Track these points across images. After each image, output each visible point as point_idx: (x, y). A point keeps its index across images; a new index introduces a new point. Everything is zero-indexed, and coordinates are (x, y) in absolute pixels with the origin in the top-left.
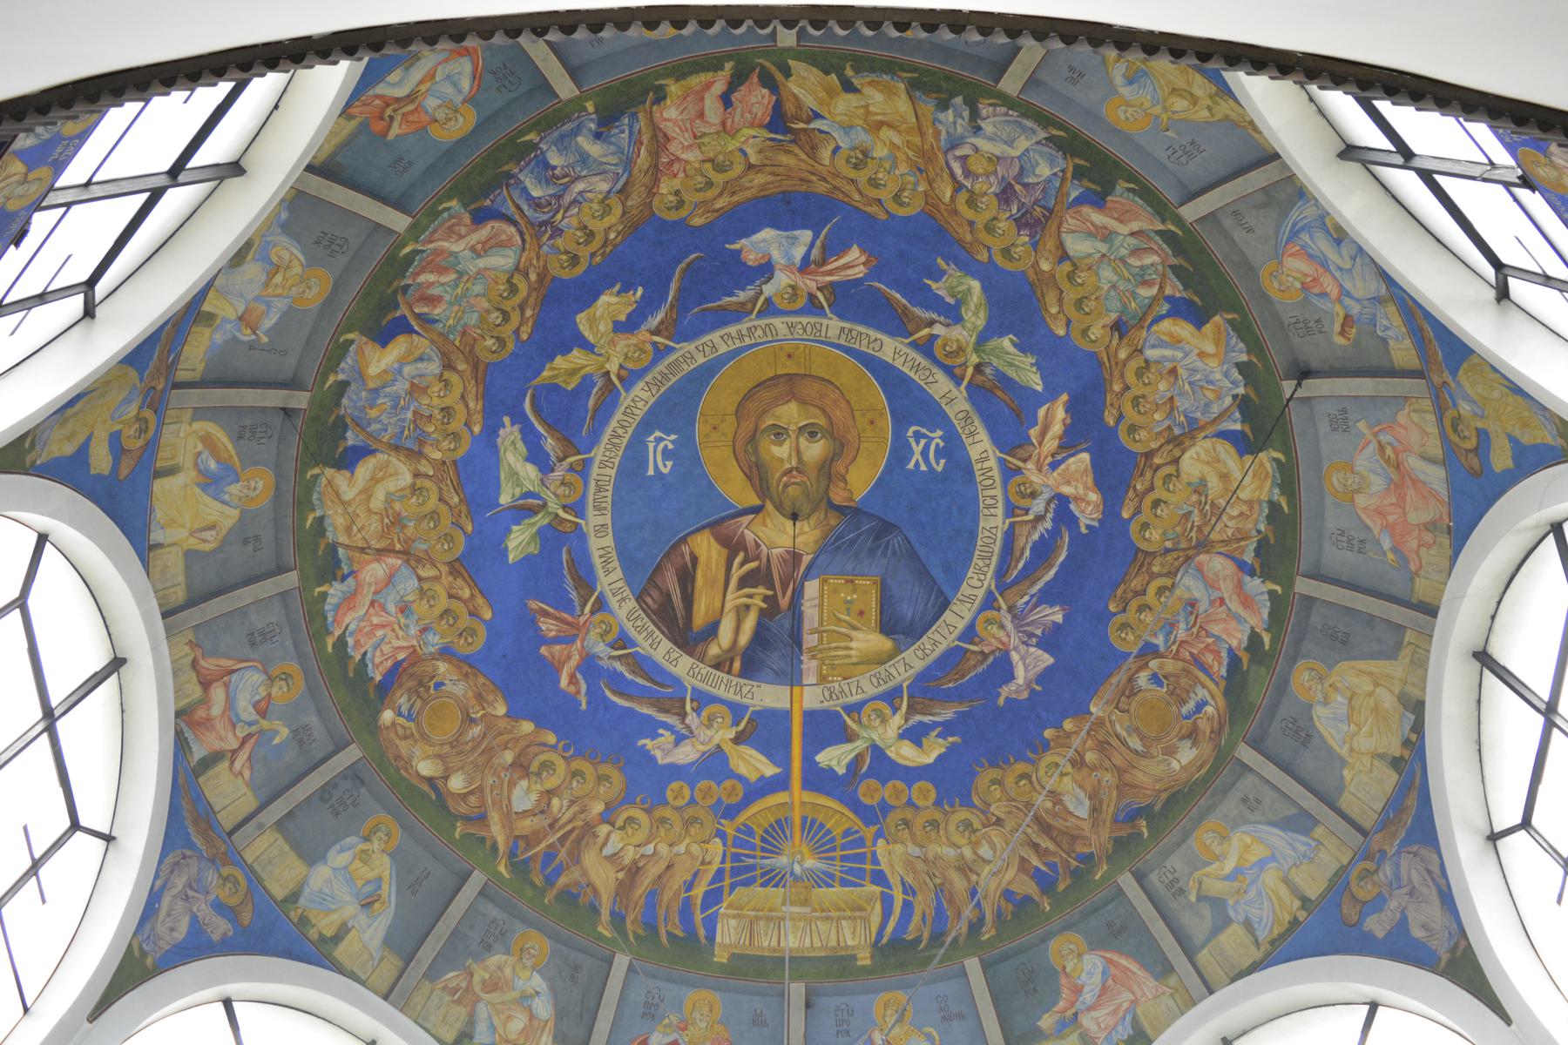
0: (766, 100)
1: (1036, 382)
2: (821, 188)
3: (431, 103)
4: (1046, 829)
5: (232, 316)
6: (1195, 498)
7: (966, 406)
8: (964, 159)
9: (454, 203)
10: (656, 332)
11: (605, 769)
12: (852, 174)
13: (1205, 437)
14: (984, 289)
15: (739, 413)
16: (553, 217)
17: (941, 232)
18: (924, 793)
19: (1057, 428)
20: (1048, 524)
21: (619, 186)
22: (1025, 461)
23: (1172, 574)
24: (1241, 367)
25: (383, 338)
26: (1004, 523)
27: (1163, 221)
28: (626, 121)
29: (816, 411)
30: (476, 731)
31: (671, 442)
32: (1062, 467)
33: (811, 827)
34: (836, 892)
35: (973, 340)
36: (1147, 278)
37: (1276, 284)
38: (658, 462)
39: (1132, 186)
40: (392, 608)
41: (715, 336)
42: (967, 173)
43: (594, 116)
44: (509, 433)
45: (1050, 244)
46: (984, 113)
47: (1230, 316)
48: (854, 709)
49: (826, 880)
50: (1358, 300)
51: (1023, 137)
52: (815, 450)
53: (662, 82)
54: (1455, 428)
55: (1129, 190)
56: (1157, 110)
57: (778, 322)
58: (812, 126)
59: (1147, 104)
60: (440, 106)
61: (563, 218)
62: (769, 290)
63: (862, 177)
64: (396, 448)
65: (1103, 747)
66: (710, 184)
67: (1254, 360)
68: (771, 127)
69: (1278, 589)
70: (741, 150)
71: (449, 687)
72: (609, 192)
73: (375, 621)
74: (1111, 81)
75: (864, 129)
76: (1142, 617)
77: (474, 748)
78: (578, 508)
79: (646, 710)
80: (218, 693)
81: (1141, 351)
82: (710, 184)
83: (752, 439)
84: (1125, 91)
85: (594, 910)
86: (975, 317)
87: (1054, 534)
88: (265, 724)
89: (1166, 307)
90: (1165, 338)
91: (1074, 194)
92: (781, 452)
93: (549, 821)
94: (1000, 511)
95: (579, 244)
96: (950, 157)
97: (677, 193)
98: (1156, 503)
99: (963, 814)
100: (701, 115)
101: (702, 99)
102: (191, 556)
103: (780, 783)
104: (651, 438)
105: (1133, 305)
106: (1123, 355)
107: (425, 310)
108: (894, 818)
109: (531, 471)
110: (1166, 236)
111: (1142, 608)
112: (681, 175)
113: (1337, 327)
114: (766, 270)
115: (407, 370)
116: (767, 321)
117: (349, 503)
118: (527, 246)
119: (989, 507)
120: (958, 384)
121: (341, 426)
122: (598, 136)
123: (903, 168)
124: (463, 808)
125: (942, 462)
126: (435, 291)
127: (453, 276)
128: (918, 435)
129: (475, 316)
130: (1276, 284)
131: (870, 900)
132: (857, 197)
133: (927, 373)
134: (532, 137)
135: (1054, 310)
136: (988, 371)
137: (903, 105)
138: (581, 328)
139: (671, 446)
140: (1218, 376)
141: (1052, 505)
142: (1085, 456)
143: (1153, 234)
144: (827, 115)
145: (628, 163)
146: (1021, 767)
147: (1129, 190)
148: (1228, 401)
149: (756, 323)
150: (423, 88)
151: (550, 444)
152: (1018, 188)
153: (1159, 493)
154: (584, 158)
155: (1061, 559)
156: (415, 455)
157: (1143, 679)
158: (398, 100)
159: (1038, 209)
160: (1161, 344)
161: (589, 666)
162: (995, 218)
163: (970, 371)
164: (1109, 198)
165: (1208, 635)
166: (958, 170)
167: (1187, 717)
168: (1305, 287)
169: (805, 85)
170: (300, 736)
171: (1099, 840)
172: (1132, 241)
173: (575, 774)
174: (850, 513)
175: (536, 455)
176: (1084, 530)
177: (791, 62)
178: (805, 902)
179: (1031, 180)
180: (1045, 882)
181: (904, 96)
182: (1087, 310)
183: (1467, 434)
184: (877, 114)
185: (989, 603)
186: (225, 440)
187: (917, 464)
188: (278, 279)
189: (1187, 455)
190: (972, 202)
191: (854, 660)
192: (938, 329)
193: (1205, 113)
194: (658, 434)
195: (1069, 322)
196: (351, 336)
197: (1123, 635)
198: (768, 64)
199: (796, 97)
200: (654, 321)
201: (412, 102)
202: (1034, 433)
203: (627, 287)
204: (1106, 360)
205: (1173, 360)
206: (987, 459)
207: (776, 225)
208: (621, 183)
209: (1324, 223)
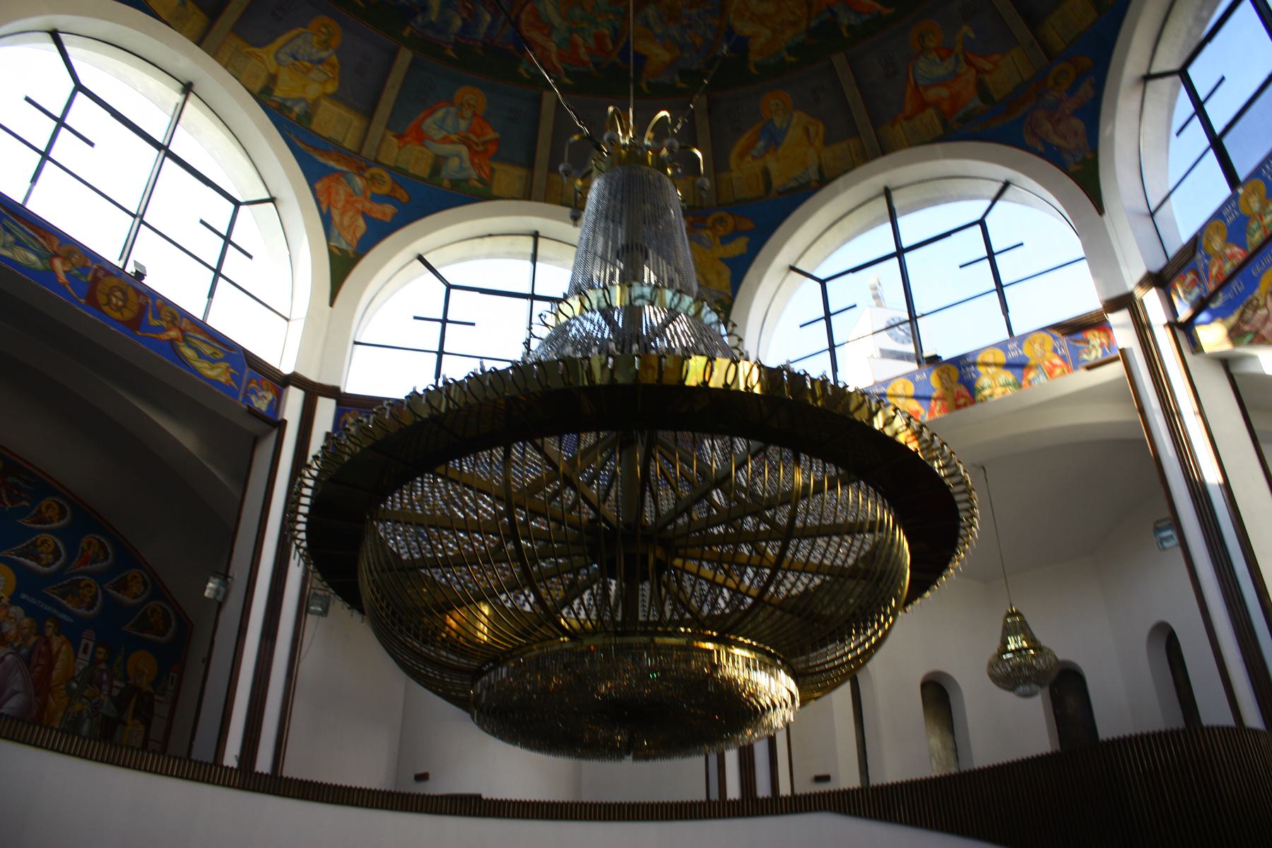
3: (463, 125)
25: (641, 59)
60: (464, 118)
80: (932, 94)
102: (827, 142)
107: (609, 42)
115: (659, 31)
126: (592, 42)
150: (454, 137)
158: (470, 148)
201: (468, 138)
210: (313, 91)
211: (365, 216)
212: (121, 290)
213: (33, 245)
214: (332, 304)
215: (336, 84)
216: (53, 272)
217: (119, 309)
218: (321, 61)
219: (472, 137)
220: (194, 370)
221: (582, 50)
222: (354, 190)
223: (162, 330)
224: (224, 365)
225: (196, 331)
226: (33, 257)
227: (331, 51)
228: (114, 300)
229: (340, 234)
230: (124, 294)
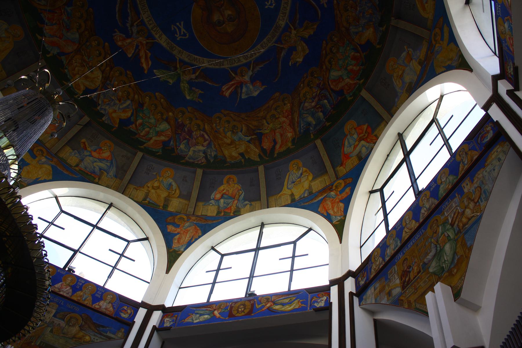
0: (264, 144)
3: (355, 136)
5: (414, 61)
6: (90, 64)
7: (175, 53)
8: (205, 140)
9: (349, 99)
13: (99, 86)
14: (186, 97)
16: (320, 92)
19: (143, 60)
20: (128, 25)
21: (302, 105)
22: (147, 43)
24: (103, 115)
26: (142, 17)
27: (145, 147)
28: (302, 131)
31: (267, 5)
32: (134, 48)
35: (182, 77)
36: (142, 126)
37: (108, 144)
39: (158, 154)
42: (203, 136)
43: (311, 132)
46: (204, 159)
47: (114, 129)
50: (86, 156)
51: (191, 155)
52: (216, 17)
53: (293, 147)
54: (41, 150)
55: (158, 152)
56: (161, 179)
58: (250, 138)
59: (164, 179)
60: (353, 135)
61: (317, 91)
62: (250, 73)
67: (101, 120)
68: (261, 134)
69: (48, 56)
70: (268, 124)
72: (305, 102)
74: (175, 182)
75: (235, 141)
76: (80, 13)
81: (132, 101)
82: (276, 109)
84: (171, 180)
86: (184, 86)
89: (132, 119)
90: (128, 110)
91: (172, 143)
92: (228, 12)
94: (146, 20)
95: (311, 81)
96: (209, 139)
97: (285, 104)
98: (100, 54)
100: (281, 135)
101: (282, 141)
104: (274, 5)
105: (141, 115)
106: (136, 96)
107: (356, 54)
110: (143, 143)
112: (284, 111)
113: (87, 144)
114: (253, 80)
116: (248, 60)
118: (327, 80)
120: (180, 60)
122: (309, 124)
123: (221, 130)
125: (173, 29)
126: (354, 62)
127: (349, 68)
128: (185, 35)
129: (341, 51)
130: (108, 144)
132: (232, 115)
133: (191, 59)
134: (328, 124)
135: (162, 100)
137: (226, 153)
138: (306, 47)
139: (266, 3)
140: (107, 108)
141: (130, 32)
142: (130, 56)
143: (146, 141)
144: (246, 143)
147: (158, 152)
148: (100, 102)
149: (251, 59)
152: (188, 137)
155: (117, 16)
158: (363, 140)
159: (180, 132)
160: (127, 107)
162: (190, 123)
163: (178, 66)
164: (162, 146)
166: (206, 136)
168: (101, 149)
169: (254, 153)
172: (150, 136)
176: (116, 30)
177: (259, 160)
181: (227, 156)
182: (153, 106)
183: (38, 153)
184: (233, 147)
186: (418, 6)
187: (180, 24)
188: (400, 72)
189: (101, 77)
190: (198, 126)
192: (193, 76)
193: (149, 185)
194: (272, 7)
195: (156, 98)
196: (378, 47)
197: (81, 2)
198: (265, 158)
199: (256, 147)
201: (360, 138)
202: (149, 54)
204: (140, 92)
206: (159, 37)
207: (254, 97)
208: (302, 106)
209: (106, 172)
210: (306, 185)
211: (341, 201)
212: (242, 305)
213: (206, 312)
214: (341, 243)
215: (311, 174)
216: (215, 316)
217: (243, 311)
218: (301, 174)
219: (361, 135)
220: (282, 312)
221: (355, 68)
222: (333, 197)
223: (264, 306)
224: (296, 301)
225: (279, 297)
226: (206, 316)
227: (301, 168)
228: (240, 310)
229: (335, 216)
230: (244, 305)
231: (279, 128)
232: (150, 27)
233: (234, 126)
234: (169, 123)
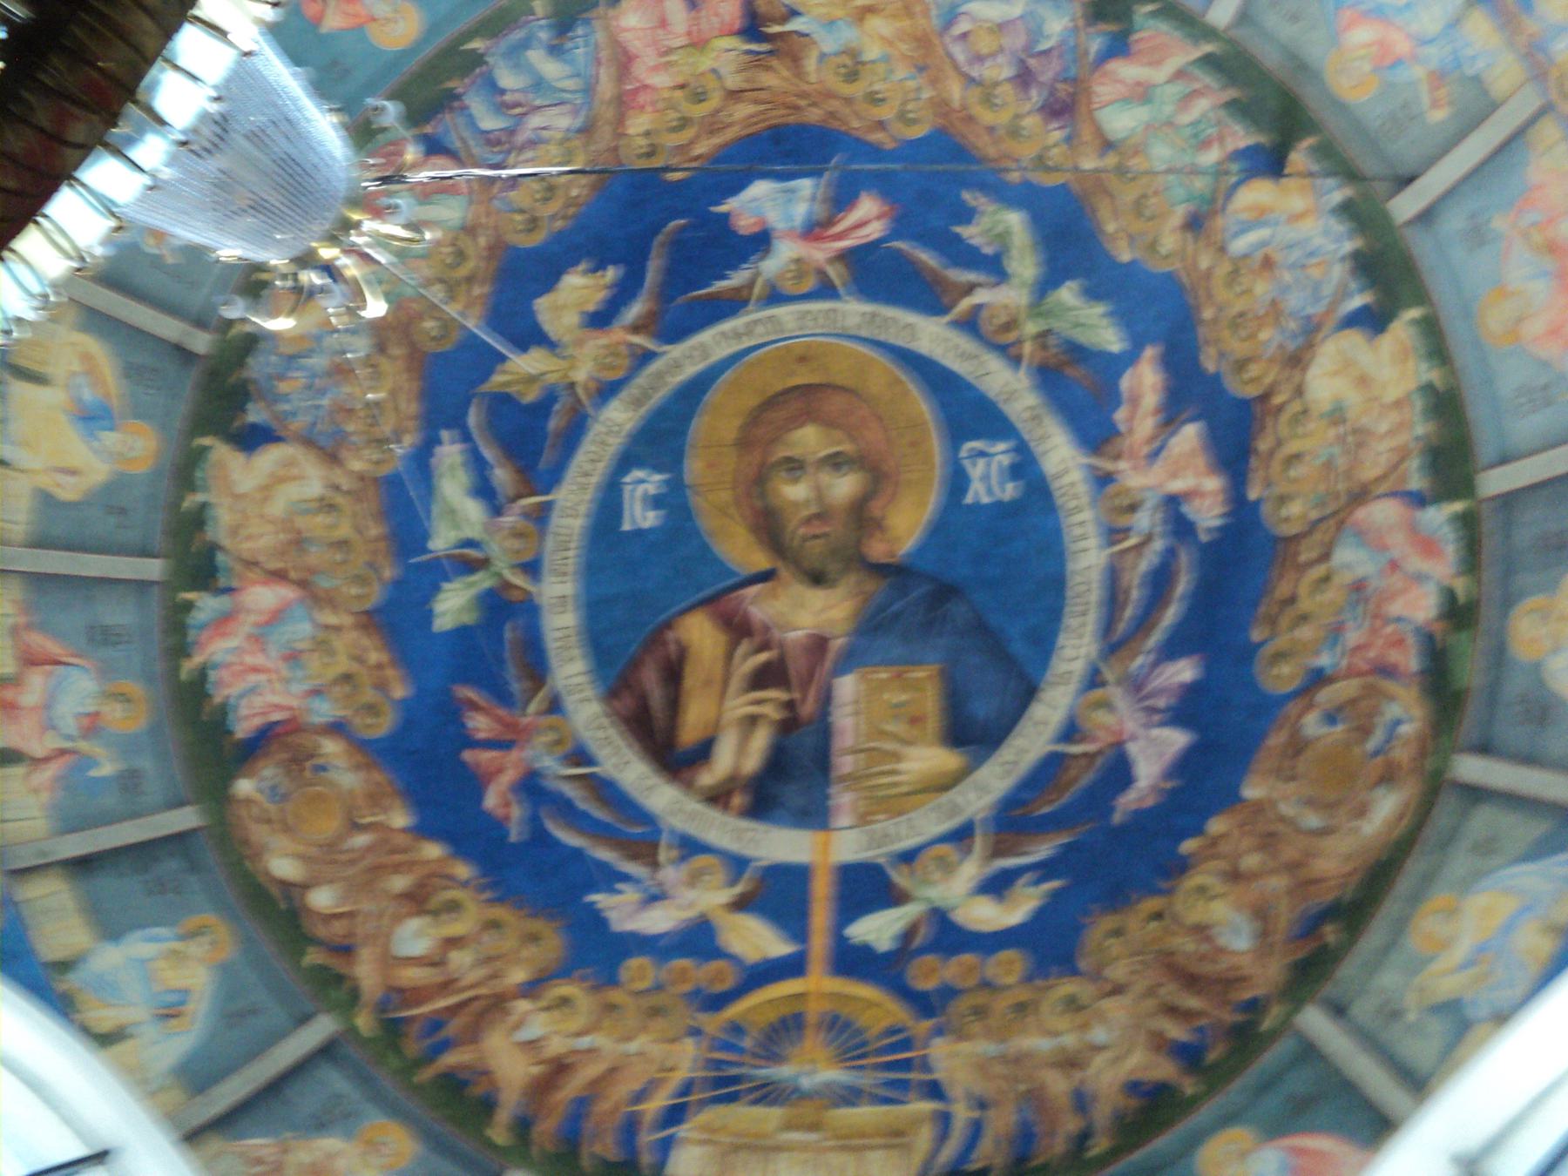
1: (1111, 339)
2: (814, 115)
4: (1191, 981)
6: (1332, 433)
10: (636, 329)
11: (538, 925)
12: (846, 89)
15: (744, 443)
17: (961, 153)
18: (1008, 966)
23: (1325, 556)
29: (838, 434)
30: (361, 840)
33: (837, 1025)
34: (865, 1114)
36: (1202, 136)
38: (640, 516)
40: (274, 651)
41: (706, 336)
44: (450, 453)
45: (1087, 134)
48: (908, 857)
49: (851, 1096)
52: (844, 486)
55: (1154, 14)
57: (784, 312)
58: (789, 27)
63: (857, 90)
64: (308, 441)
65: (1268, 842)
66: (684, 123)
71: (332, 775)
73: (249, 660)
77: (352, 862)
78: (532, 568)
79: (604, 854)
81: (1222, 250)
83: (760, 480)
85: (488, 1106)
86: (1025, 266)
87: (1170, 553)
88: (83, 745)
92: (795, 492)
93: (440, 979)
94: (1093, 542)
97: (647, 134)
99: (1068, 987)
100: (663, 23)
103: (793, 967)
108: (962, 1005)
109: (473, 510)
110: (1208, 61)
111: (1304, 618)
114: (761, 241)
117: (238, 497)
119: (1084, 537)
121: (240, 395)
122: (555, 51)
123: (901, 72)
124: (321, 931)
131: (916, 1121)
134: (477, 44)
136: (1052, 341)
145: (589, 90)
146: (1152, 904)
151: (502, 476)
152: (1032, 62)
153: (1293, 447)
154: (539, 84)
156: (332, 457)
157: (1312, 724)
160: (1246, 228)
161: (531, 786)
165: (1387, 621)
167: (1376, 753)
170: (129, 781)
171: (1268, 975)
173: (494, 925)
174: (895, 573)
175: (484, 490)
178: (814, 1127)
179: (1044, 45)
180: (1188, 1055)
185: (1094, 680)
191: (904, 789)
192: (980, 297)
200: (635, 310)
202: (1120, 415)
203: (600, 267)
205: (1264, 244)
231: (670, 51)
232: (1087, 515)
233: (852, 76)
234: (1099, 132)
